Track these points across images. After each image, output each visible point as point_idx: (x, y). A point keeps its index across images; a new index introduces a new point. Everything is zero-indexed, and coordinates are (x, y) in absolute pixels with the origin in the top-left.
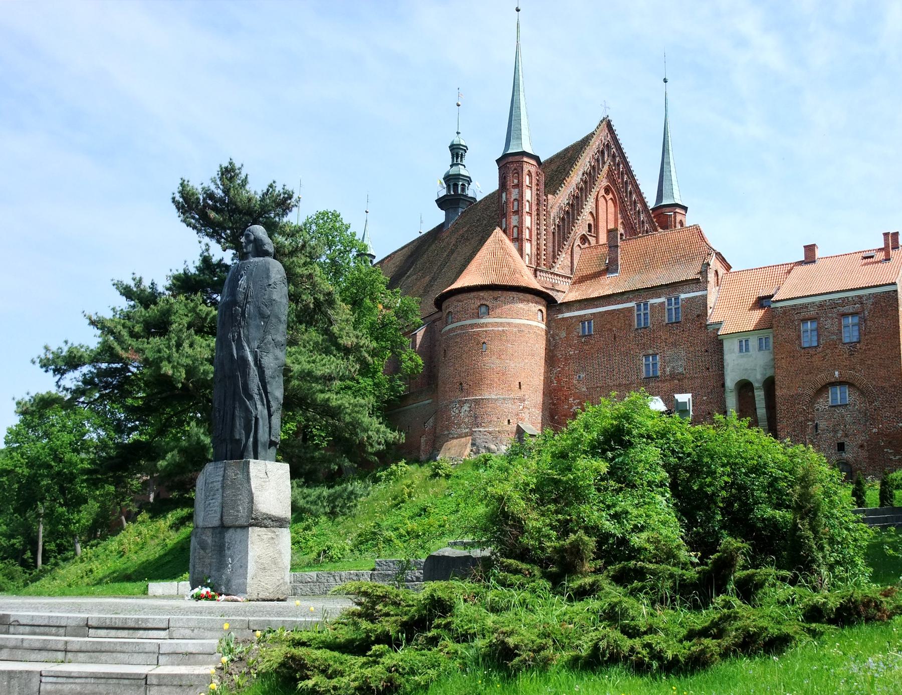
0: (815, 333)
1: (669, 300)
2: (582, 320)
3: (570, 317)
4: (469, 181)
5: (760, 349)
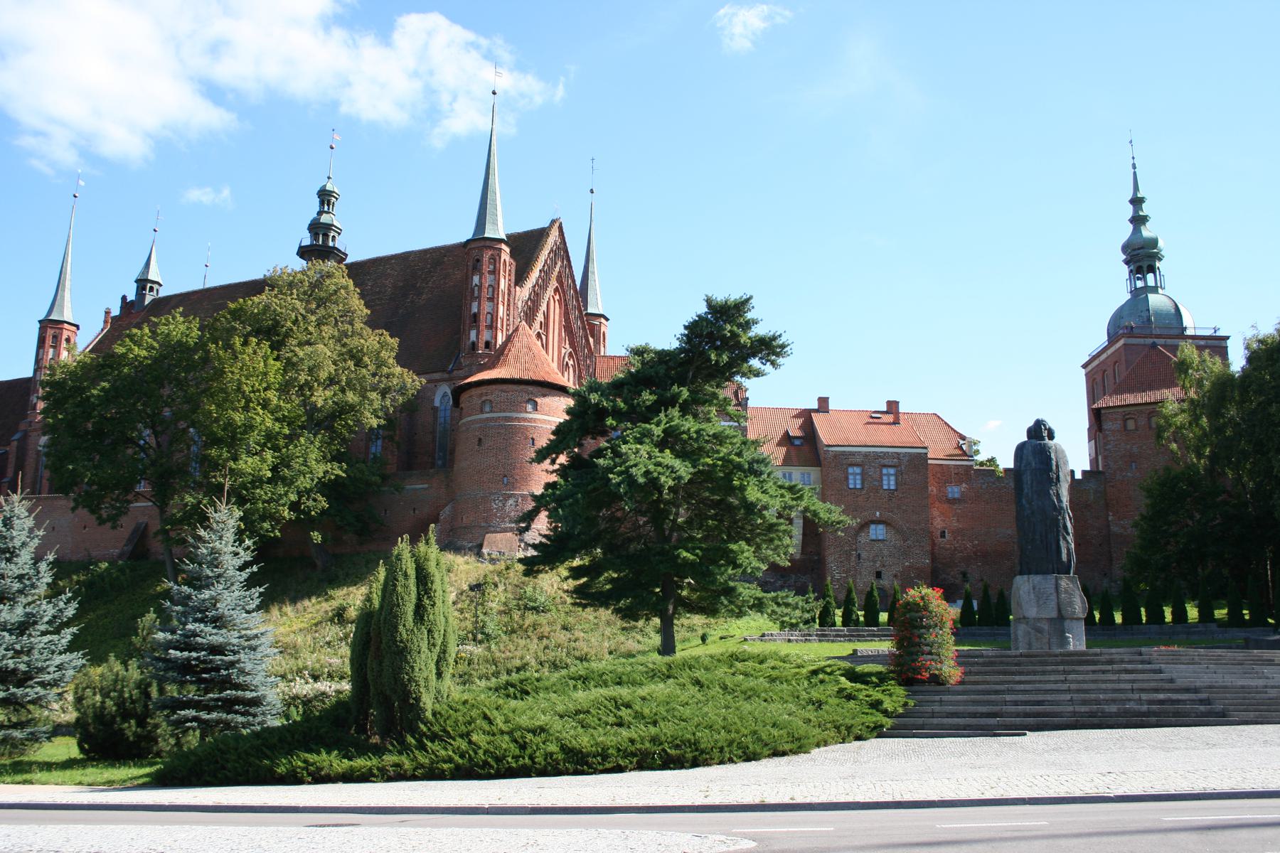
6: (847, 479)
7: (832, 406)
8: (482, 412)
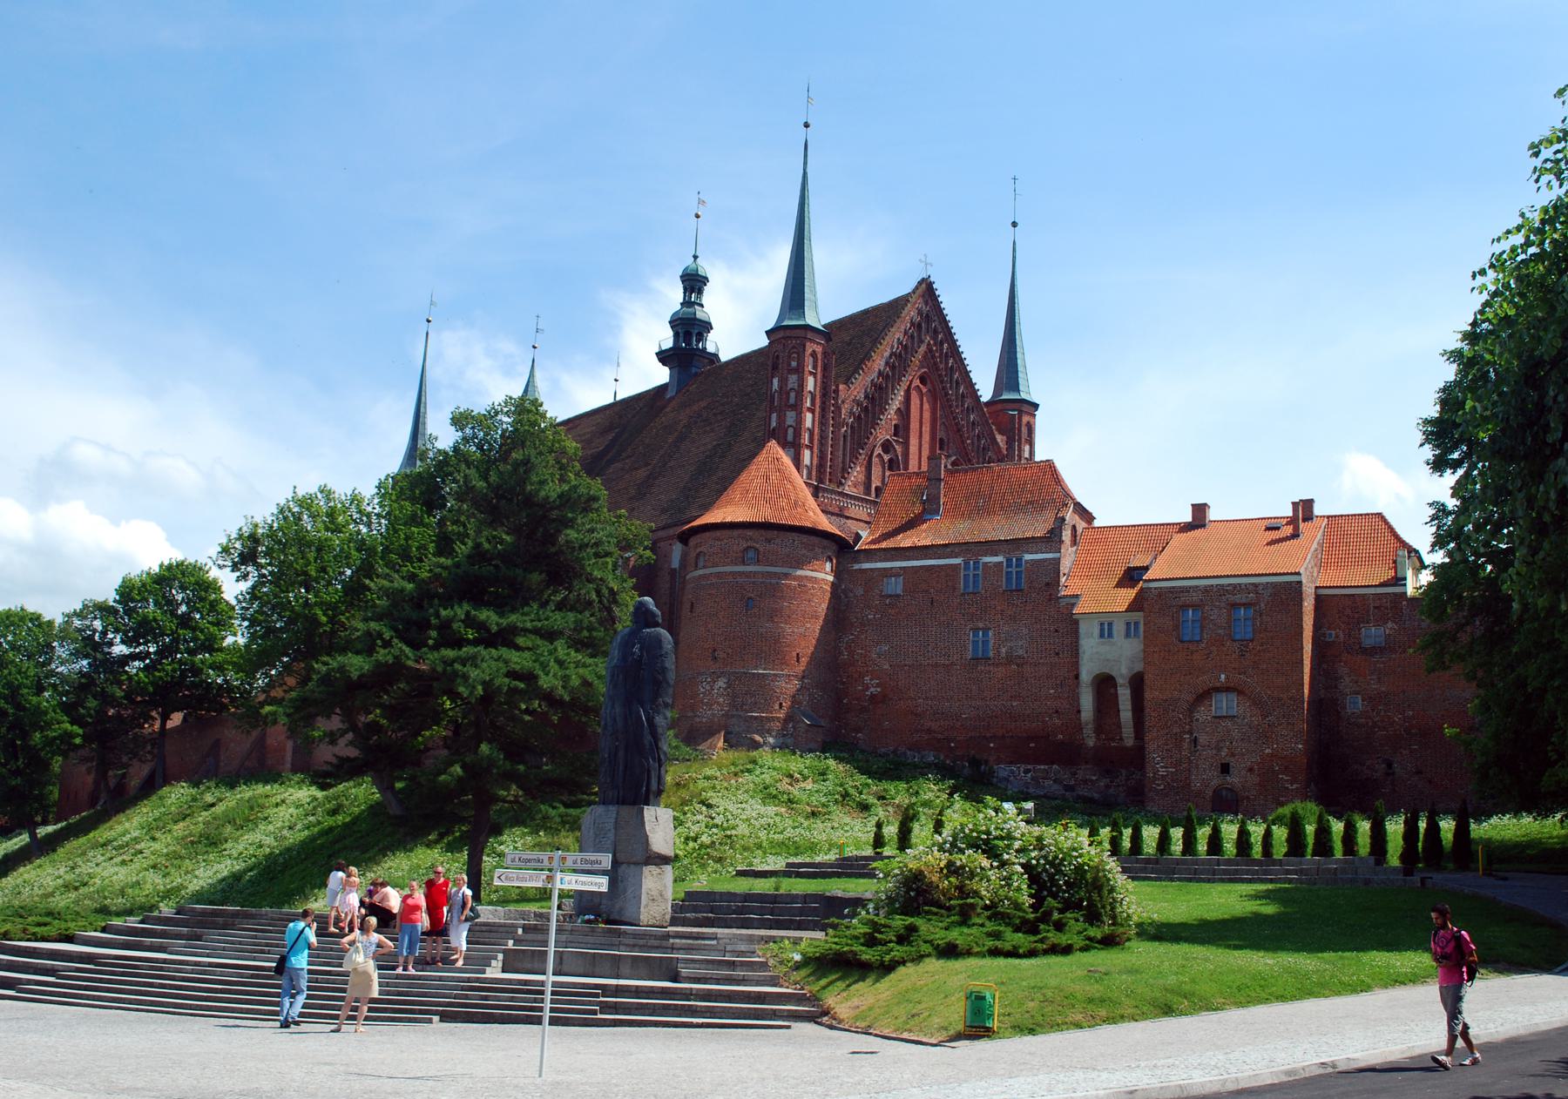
0: (1197, 625)
1: (1009, 561)
2: (887, 573)
4: (707, 326)
5: (1128, 635)
6: (1176, 627)
7: (1213, 515)
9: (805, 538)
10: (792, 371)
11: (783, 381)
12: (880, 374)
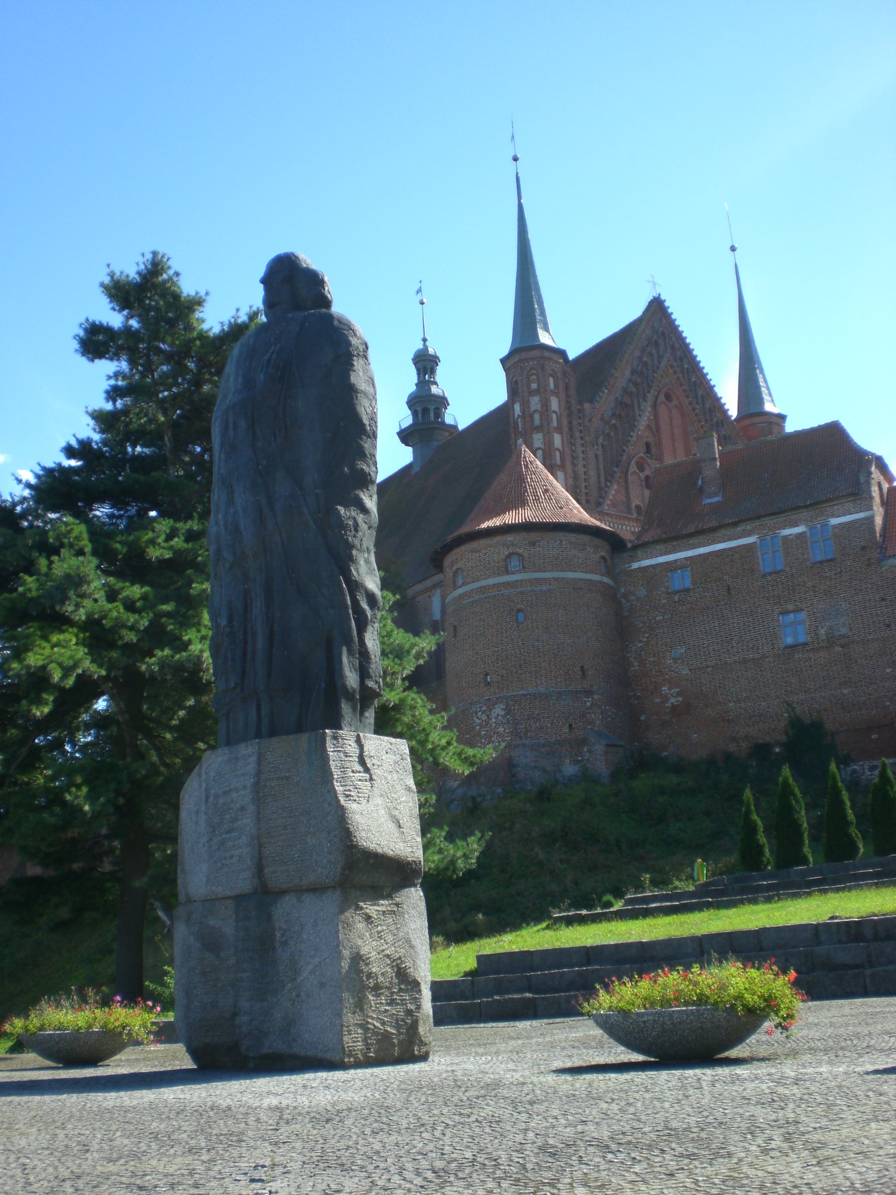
3: (652, 566)
8: (455, 587)
9: (573, 537)
10: (532, 393)
11: (525, 405)
12: (625, 390)
